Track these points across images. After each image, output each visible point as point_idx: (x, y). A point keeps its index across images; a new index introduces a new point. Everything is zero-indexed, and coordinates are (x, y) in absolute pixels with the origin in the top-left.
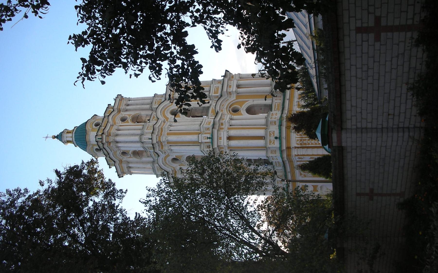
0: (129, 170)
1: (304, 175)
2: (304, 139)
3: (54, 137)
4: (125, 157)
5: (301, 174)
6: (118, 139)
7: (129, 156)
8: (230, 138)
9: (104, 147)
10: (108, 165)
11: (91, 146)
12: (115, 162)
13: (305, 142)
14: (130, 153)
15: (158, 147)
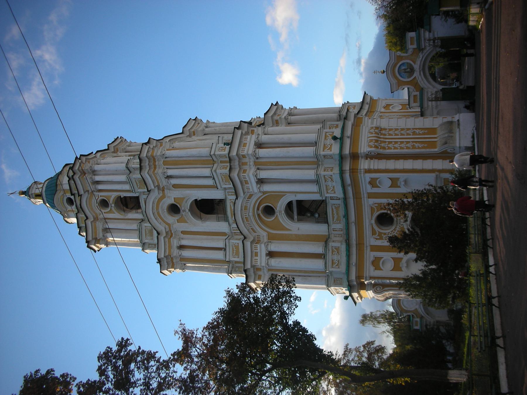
0: (105, 235)
1: (380, 234)
2: (382, 140)
3: (23, 193)
4: (103, 211)
5: (374, 232)
6: (96, 167)
7: (109, 210)
8: (259, 145)
9: (74, 177)
10: (78, 228)
11: (62, 193)
12: (87, 218)
13: (383, 145)
14: (111, 202)
15: (148, 169)
